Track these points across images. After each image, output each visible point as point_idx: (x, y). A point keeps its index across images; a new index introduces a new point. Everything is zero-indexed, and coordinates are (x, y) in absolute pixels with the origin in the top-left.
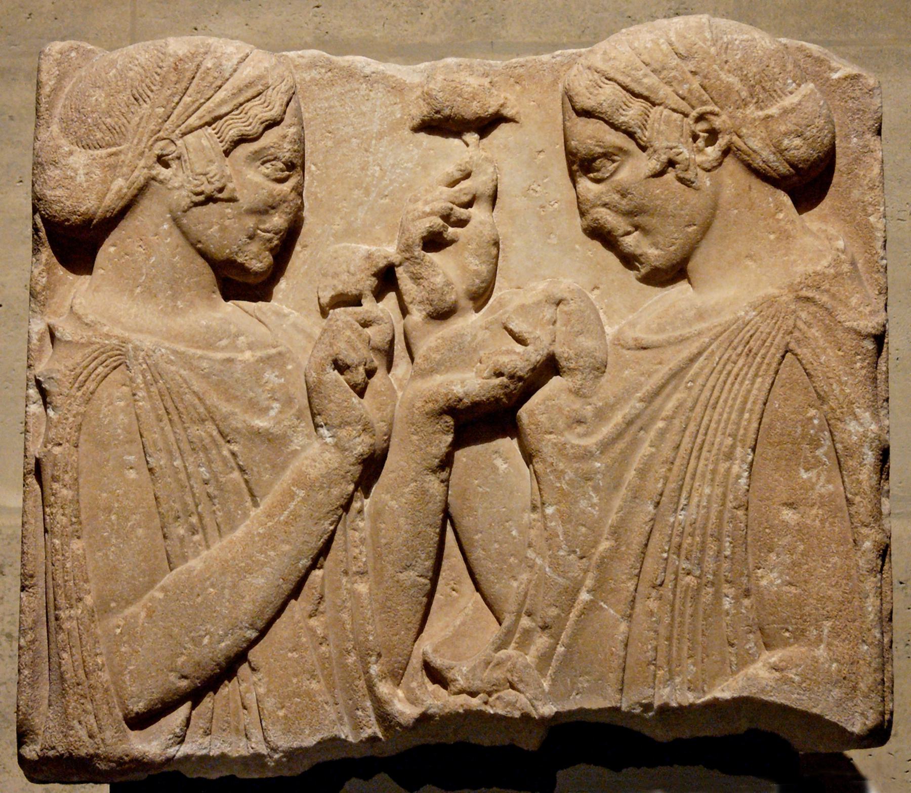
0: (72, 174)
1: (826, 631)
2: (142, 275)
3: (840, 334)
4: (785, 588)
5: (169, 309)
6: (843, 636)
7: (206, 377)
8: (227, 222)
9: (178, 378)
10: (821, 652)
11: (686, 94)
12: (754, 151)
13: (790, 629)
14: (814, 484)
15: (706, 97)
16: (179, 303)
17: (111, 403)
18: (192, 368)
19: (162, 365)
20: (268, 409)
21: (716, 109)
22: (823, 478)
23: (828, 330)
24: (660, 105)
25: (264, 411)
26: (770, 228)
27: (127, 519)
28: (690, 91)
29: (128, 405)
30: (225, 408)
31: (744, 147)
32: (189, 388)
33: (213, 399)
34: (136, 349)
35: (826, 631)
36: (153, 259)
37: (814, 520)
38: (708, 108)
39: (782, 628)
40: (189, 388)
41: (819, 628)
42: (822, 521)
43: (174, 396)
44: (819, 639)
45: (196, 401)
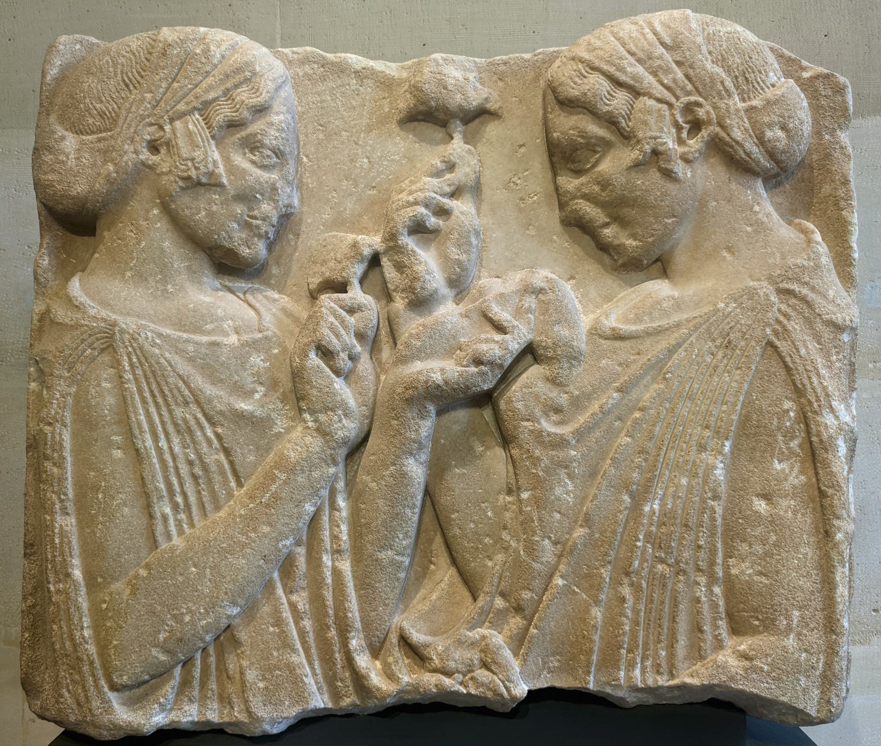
0: (64, 159)
1: (795, 621)
2: (132, 259)
3: (819, 326)
4: (755, 578)
5: (159, 293)
6: (812, 626)
7: (191, 360)
8: (215, 208)
9: (162, 361)
10: (791, 642)
11: (671, 84)
12: (737, 142)
13: (760, 617)
14: (787, 475)
15: (690, 87)
16: (169, 287)
17: (99, 385)
18: (179, 352)
19: (147, 346)
20: (254, 391)
21: (701, 100)
22: (796, 470)
23: (809, 323)
24: (644, 94)
25: (248, 394)
26: (748, 220)
27: (113, 498)
28: (675, 80)
29: (115, 387)
30: (210, 390)
31: (727, 139)
32: (174, 371)
33: (198, 380)
34: (122, 331)
35: (795, 621)
36: (143, 244)
37: (786, 512)
38: (693, 98)
39: (752, 617)
40: (174, 371)
41: (788, 617)
42: (795, 513)
43: (159, 379)
44: (789, 629)
45: (181, 384)
